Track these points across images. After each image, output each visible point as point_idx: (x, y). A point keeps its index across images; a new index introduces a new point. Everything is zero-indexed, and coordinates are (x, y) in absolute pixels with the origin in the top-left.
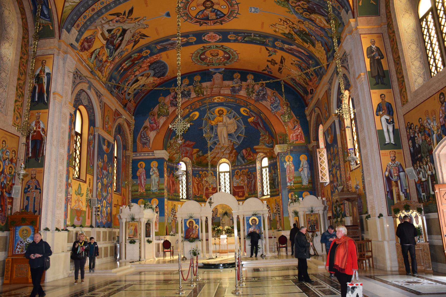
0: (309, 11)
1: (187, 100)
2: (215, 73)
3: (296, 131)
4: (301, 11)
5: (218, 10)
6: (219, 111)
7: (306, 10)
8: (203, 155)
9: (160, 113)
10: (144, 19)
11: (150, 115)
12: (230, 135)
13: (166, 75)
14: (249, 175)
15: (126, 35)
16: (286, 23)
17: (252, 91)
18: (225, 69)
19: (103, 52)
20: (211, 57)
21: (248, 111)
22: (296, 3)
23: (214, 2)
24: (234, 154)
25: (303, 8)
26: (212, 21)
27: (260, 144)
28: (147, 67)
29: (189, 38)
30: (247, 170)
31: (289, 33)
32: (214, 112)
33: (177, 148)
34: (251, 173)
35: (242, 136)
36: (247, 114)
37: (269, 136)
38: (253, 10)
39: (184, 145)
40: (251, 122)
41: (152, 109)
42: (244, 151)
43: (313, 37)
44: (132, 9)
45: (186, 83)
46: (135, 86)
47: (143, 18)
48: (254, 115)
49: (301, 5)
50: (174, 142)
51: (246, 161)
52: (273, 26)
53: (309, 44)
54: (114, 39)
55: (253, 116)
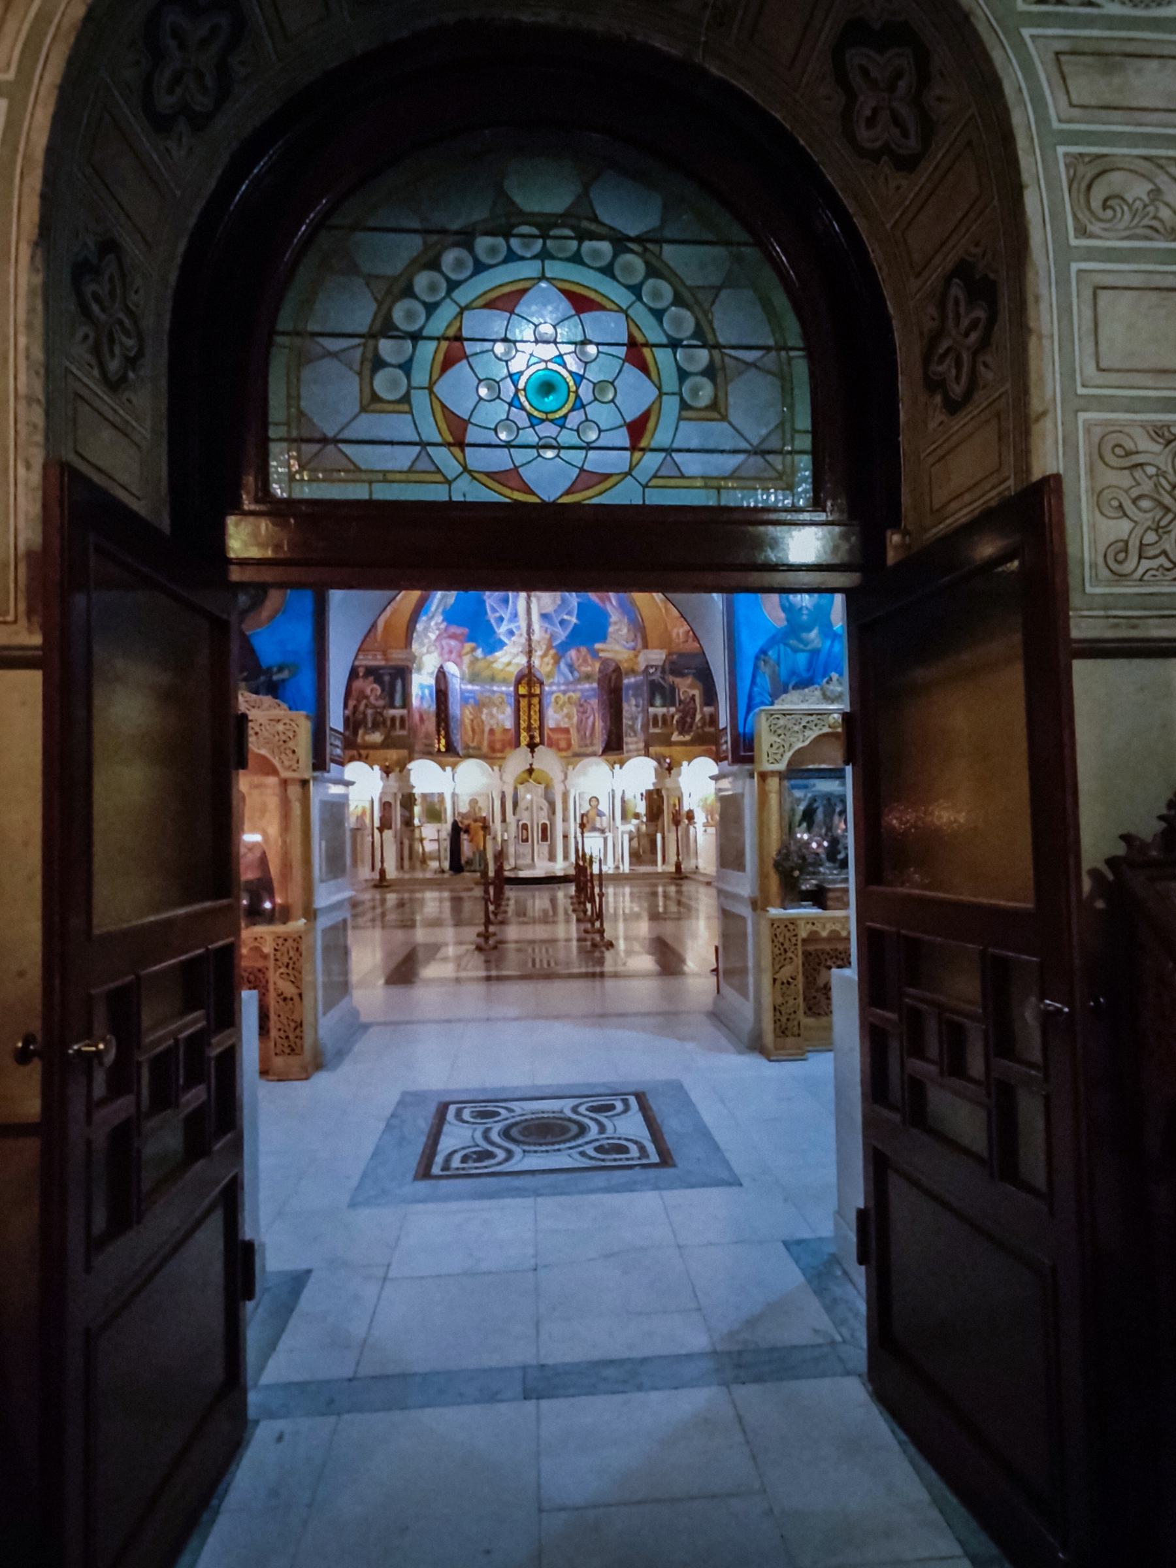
8: (485, 658)
14: (581, 706)
30: (578, 694)
34: (586, 701)
35: (569, 622)
39: (445, 635)
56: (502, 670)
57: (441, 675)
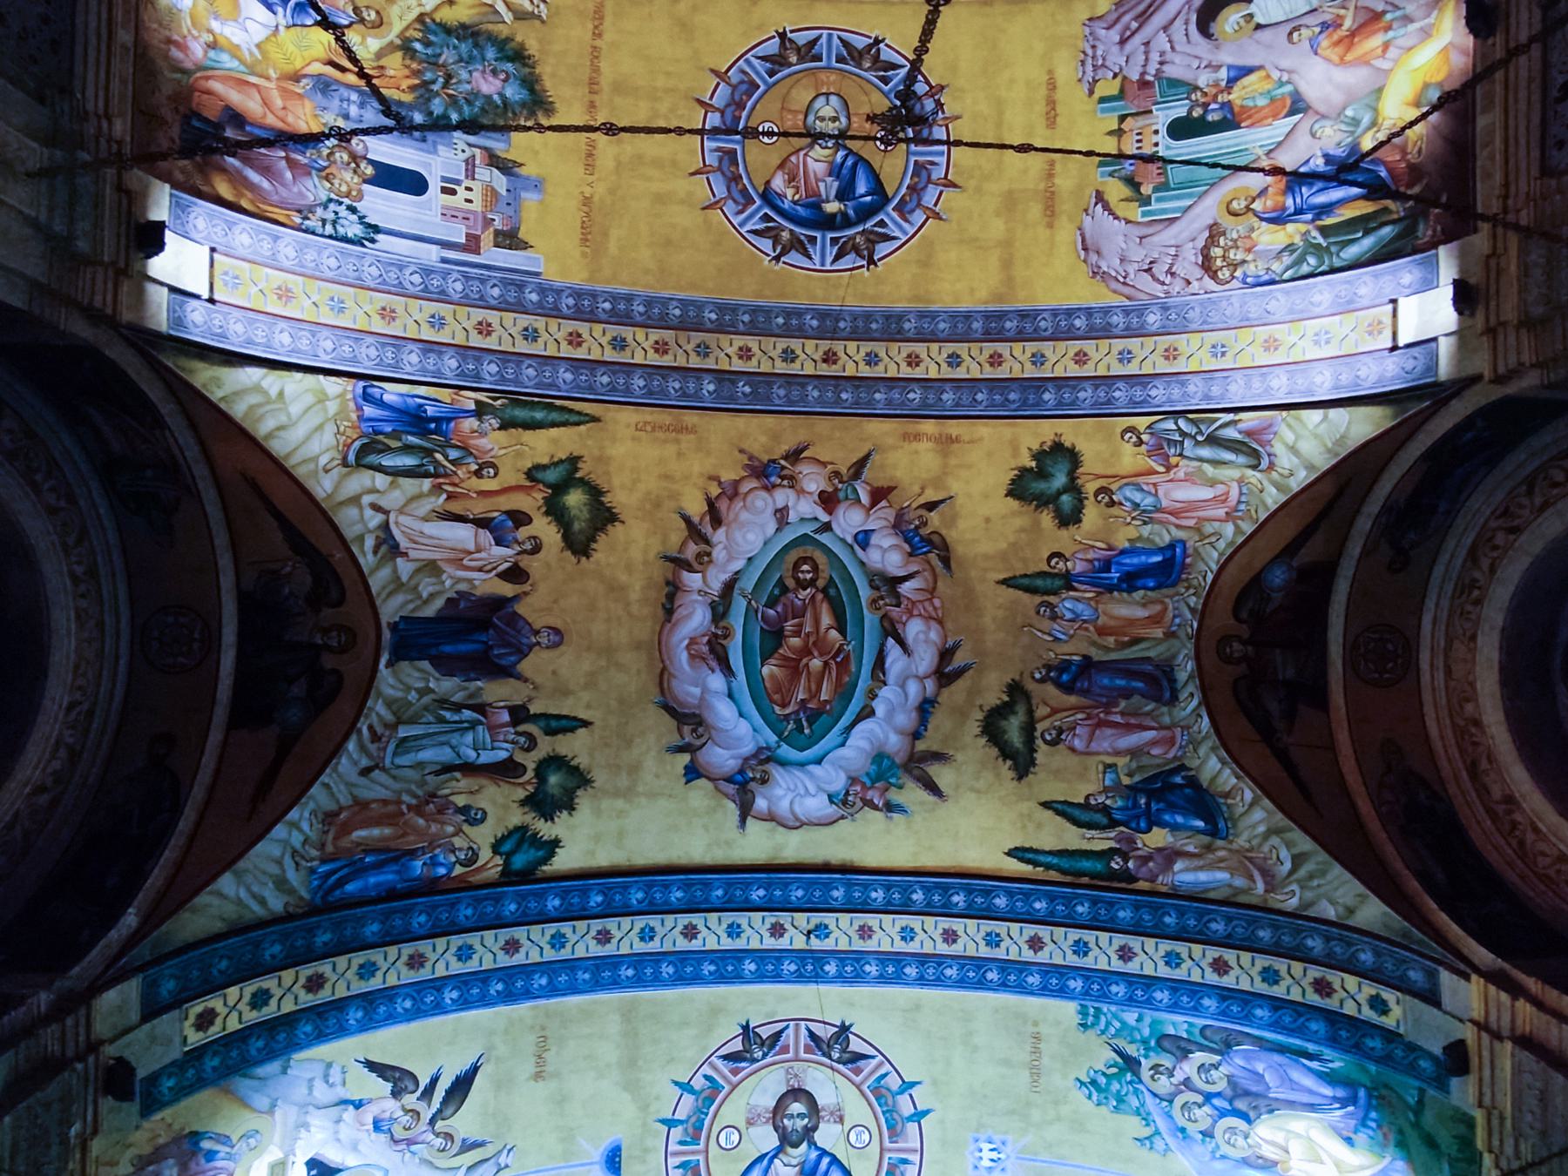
0: (1241, 1105)
4: (1203, 1114)
5: (835, 1160)
7: (1226, 1105)
10: (502, 1160)
23: (820, 1102)
25: (1208, 1097)
38: (986, 1155)
44: (474, 1070)
47: (500, 1152)
49: (1198, 1082)
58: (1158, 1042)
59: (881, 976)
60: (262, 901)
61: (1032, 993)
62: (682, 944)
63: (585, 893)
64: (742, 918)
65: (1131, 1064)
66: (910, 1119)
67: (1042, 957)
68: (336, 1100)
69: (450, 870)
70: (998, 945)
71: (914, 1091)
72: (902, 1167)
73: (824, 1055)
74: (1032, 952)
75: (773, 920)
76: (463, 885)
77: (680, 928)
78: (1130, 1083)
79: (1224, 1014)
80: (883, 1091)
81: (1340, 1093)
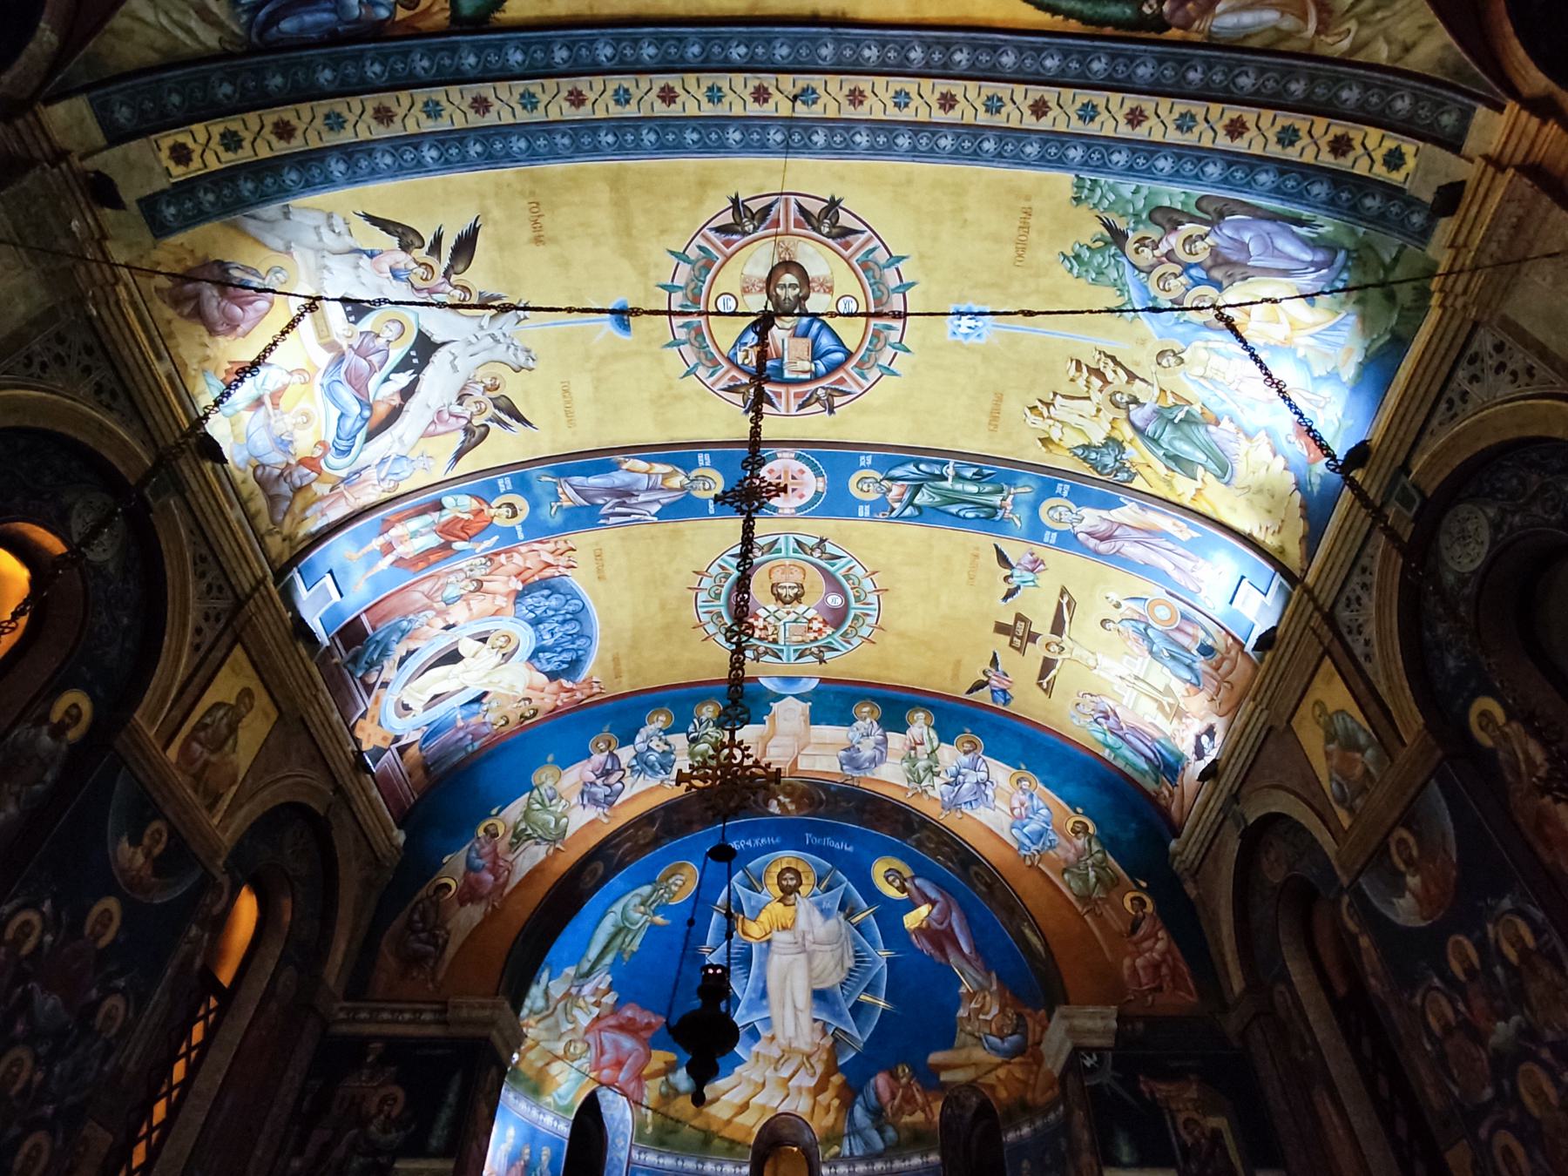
0: (1217, 274)
1: (653, 782)
2: (780, 697)
3: (1146, 945)
6: (780, 876)
7: (1203, 275)
9: (526, 830)
11: (481, 833)
12: (820, 996)
13: (584, 675)
15: (429, 372)
16: (1096, 383)
17: (929, 769)
18: (822, 680)
19: (303, 405)
20: (772, 608)
21: (907, 872)
22: (1156, 247)
23: (811, 274)
24: (837, 1097)
25: (1187, 267)
26: (794, 390)
27: (957, 1043)
28: (507, 595)
29: (693, 474)
31: (1113, 443)
32: (760, 880)
33: (573, 1029)
36: (902, 889)
37: (1001, 994)
39: (612, 1021)
40: (920, 930)
41: (494, 812)
42: (881, 1081)
43: (1225, 423)
45: (660, 725)
46: (443, 679)
48: (933, 894)
49: (1181, 255)
50: (567, 994)
51: (891, 1133)
52: (1041, 414)
53: (1200, 471)
54: (372, 371)
55: (927, 900)
56: (729, 1122)
57: (589, 1118)
58: (1150, 217)
59: (872, 147)
60: (189, 31)
61: (1028, 164)
62: (661, 109)
63: (547, 46)
64: (723, 80)
65: (1118, 237)
66: (895, 290)
67: (1045, 124)
68: (348, 248)
69: (393, 13)
70: (998, 111)
71: (900, 265)
72: (886, 332)
73: (814, 229)
74: (1034, 118)
75: (757, 83)
76: (412, 32)
77: (656, 90)
78: (1113, 256)
79: (1225, 181)
80: (871, 264)
81: (1320, 257)
